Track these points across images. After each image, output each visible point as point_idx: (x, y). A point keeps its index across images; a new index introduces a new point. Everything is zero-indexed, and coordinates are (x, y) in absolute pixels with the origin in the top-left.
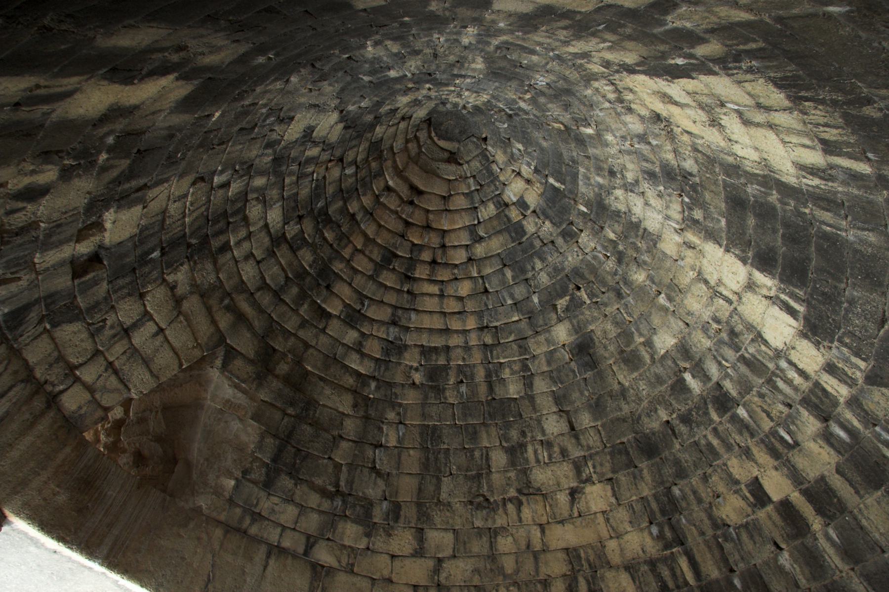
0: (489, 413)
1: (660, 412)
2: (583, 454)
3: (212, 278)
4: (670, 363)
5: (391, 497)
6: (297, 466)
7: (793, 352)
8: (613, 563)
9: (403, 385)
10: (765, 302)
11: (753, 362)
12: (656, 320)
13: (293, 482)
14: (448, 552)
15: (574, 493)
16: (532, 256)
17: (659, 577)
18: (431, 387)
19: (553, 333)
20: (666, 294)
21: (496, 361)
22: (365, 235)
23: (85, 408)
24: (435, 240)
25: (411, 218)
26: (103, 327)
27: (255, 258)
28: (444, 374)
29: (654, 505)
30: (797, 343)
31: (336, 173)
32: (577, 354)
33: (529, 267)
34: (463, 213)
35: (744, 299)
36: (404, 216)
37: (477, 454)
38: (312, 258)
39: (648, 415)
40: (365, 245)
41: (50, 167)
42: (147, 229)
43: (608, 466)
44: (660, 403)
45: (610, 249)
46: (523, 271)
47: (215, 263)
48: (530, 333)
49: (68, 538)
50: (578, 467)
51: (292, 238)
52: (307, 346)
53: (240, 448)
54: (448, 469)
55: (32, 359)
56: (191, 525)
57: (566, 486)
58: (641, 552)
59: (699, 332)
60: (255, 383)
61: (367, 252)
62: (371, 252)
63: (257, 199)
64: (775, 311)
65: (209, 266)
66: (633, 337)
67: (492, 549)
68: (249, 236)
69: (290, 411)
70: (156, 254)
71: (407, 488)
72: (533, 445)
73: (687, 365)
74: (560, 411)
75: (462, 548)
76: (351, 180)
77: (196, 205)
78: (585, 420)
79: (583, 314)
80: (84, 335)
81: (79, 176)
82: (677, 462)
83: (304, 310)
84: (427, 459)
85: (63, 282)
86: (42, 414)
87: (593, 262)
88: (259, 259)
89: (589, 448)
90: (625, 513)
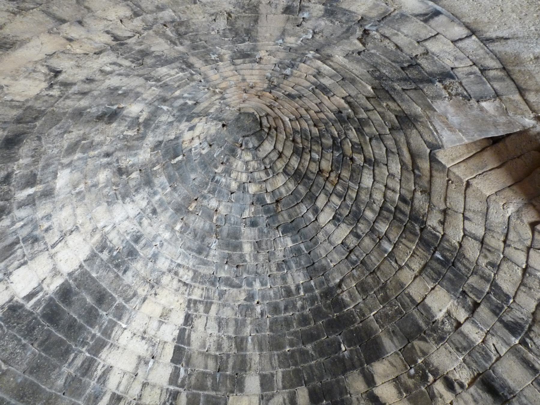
3: (418, 194)
7: (5, 287)
10: (43, 277)
11: (11, 250)
12: (77, 175)
30: (9, 293)
35: (50, 260)
41: (435, 391)
42: (433, 278)
44: (34, 162)
47: (412, 199)
64: (34, 284)
65: (416, 202)
80: (501, 273)
81: (433, 366)
85: (483, 311)
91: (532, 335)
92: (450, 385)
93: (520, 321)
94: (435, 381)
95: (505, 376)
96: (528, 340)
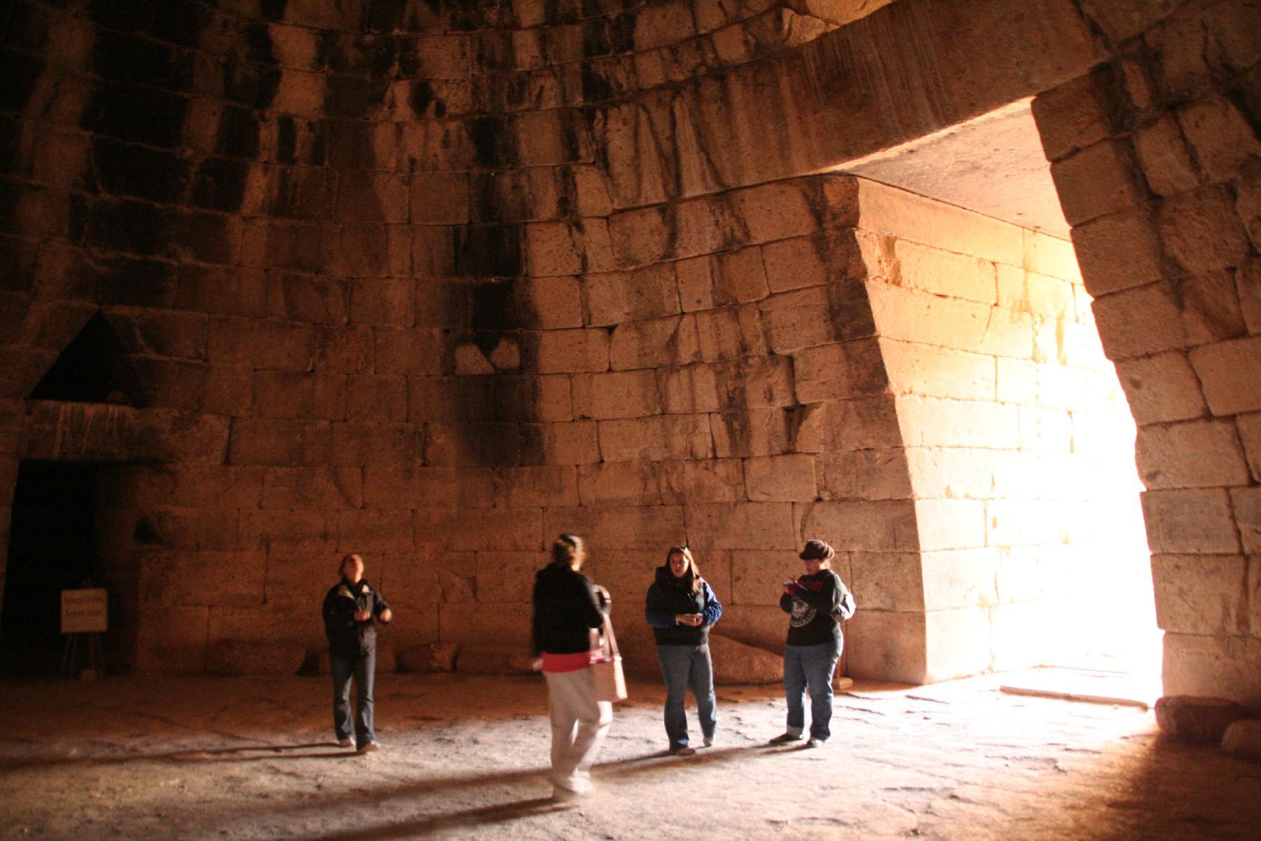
23: (750, 37)
41: (389, 94)
55: (658, 79)
91: (613, 113)
92: (422, 98)
93: (612, 83)
94: (398, 78)
95: (523, 136)
96: (599, 115)
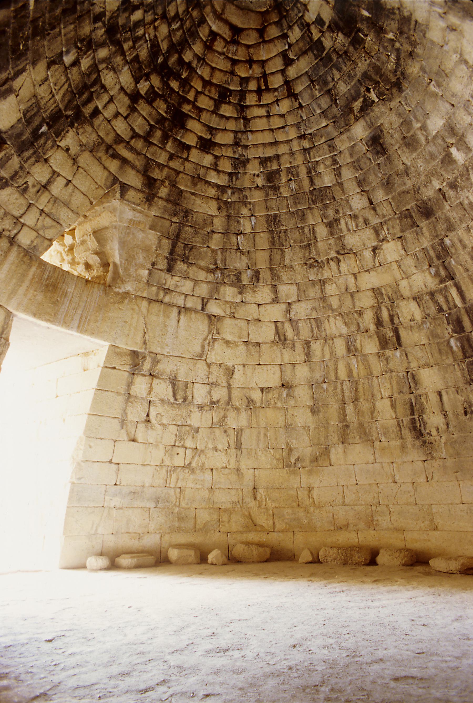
0: (312, 199)
1: (433, 182)
2: (380, 221)
4: (440, 141)
5: (252, 266)
6: (187, 255)
8: (405, 296)
9: (250, 189)
12: (428, 107)
13: (186, 265)
14: (294, 298)
15: (374, 250)
16: (331, 69)
17: (437, 303)
18: (270, 187)
19: (352, 131)
20: (436, 81)
21: (313, 160)
22: (202, 78)
23: (35, 242)
24: (257, 71)
25: (235, 55)
26: (27, 187)
27: (122, 115)
28: (277, 176)
29: (432, 253)
31: (164, 30)
32: (371, 145)
33: (330, 79)
34: (276, 41)
36: (230, 55)
37: (306, 230)
38: (165, 106)
39: (425, 186)
40: (204, 87)
43: (398, 228)
45: (389, 48)
46: (326, 83)
48: (336, 134)
49: (51, 319)
50: (377, 232)
51: (145, 94)
52: (178, 173)
53: (146, 249)
54: (288, 243)
56: (126, 301)
57: (370, 246)
58: (424, 287)
59: (462, 110)
60: (146, 205)
61: (207, 93)
62: (210, 91)
63: (107, 68)
65: (89, 129)
66: (412, 124)
67: (322, 293)
68: (111, 100)
69: (175, 219)
70: (44, 128)
71: (262, 260)
72: (344, 218)
73: (453, 141)
74: (362, 191)
75: (303, 295)
76: (179, 33)
77: (59, 85)
78: (380, 195)
79: (372, 110)
80: (17, 195)
82: (447, 220)
83: (170, 146)
84: (273, 238)
86: (9, 250)
87: (378, 63)
88: (125, 115)
89: (384, 216)
90: (412, 260)
